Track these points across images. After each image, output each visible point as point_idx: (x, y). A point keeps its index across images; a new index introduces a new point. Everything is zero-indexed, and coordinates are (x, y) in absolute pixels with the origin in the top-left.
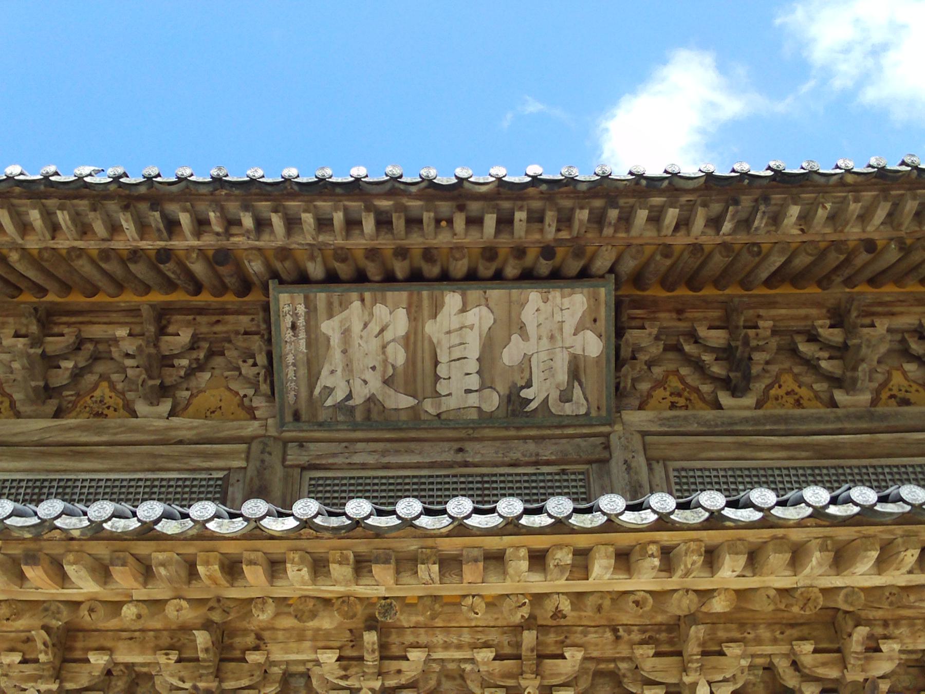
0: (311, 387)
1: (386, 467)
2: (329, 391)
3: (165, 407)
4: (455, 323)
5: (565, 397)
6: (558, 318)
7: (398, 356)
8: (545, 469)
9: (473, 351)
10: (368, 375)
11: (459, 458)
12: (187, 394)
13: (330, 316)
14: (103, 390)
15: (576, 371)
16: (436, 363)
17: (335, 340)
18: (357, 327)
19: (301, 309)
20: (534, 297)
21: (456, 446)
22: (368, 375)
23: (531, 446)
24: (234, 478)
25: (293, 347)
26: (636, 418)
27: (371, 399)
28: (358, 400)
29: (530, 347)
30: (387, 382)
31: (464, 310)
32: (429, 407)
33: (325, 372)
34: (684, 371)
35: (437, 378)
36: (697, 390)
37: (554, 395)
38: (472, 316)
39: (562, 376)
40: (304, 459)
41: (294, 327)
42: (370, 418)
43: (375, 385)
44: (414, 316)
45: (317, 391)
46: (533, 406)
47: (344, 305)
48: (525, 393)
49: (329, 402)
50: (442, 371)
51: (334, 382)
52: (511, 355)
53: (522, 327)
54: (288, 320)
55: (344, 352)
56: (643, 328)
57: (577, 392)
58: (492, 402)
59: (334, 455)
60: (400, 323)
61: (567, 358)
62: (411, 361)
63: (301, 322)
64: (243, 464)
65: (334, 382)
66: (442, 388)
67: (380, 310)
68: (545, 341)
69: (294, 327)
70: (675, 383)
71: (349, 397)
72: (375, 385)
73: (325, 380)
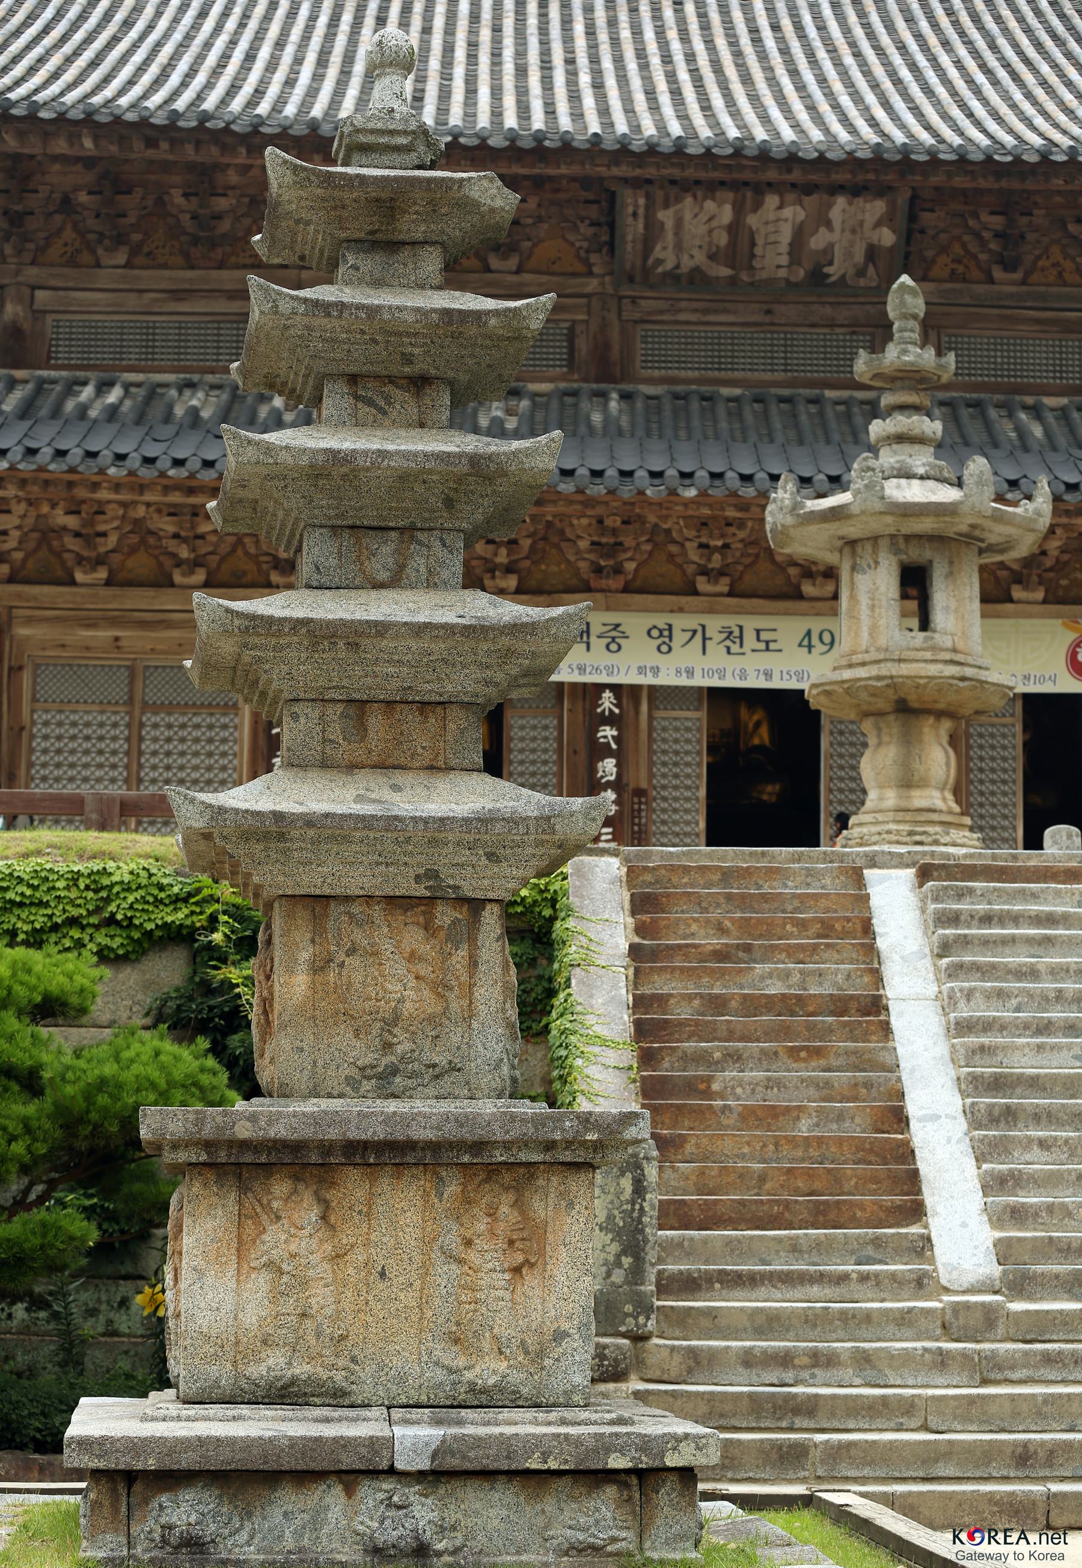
0: (645, 258)
1: (708, 323)
2: (659, 262)
3: (513, 263)
4: (772, 217)
5: (861, 273)
6: (860, 217)
7: (723, 239)
8: (838, 330)
9: (786, 236)
10: (695, 252)
11: (767, 319)
12: (528, 244)
13: (666, 206)
16: (753, 244)
17: (669, 224)
18: (688, 216)
19: (642, 201)
20: (841, 201)
21: (765, 307)
22: (695, 252)
23: (828, 310)
24: (579, 329)
25: (633, 229)
27: (696, 270)
28: (684, 269)
29: (835, 237)
30: (711, 257)
31: (781, 207)
32: (745, 277)
33: (658, 248)
34: (967, 238)
35: (753, 256)
36: (975, 257)
37: (851, 272)
38: (788, 212)
39: (859, 257)
40: (637, 316)
41: (635, 215)
43: (700, 258)
44: (739, 210)
45: (650, 261)
46: (833, 279)
47: (678, 200)
48: (826, 270)
49: (660, 270)
50: (758, 251)
51: (665, 255)
52: (818, 241)
53: (829, 224)
54: (630, 210)
55: (676, 234)
56: (932, 210)
57: (871, 270)
59: (662, 312)
60: (726, 214)
61: (864, 245)
62: (733, 243)
63: (641, 211)
64: (584, 317)
65: (665, 255)
66: (756, 263)
67: (710, 205)
68: (847, 233)
69: (635, 215)
70: (957, 249)
71: (678, 267)
72: (700, 258)
73: (658, 252)
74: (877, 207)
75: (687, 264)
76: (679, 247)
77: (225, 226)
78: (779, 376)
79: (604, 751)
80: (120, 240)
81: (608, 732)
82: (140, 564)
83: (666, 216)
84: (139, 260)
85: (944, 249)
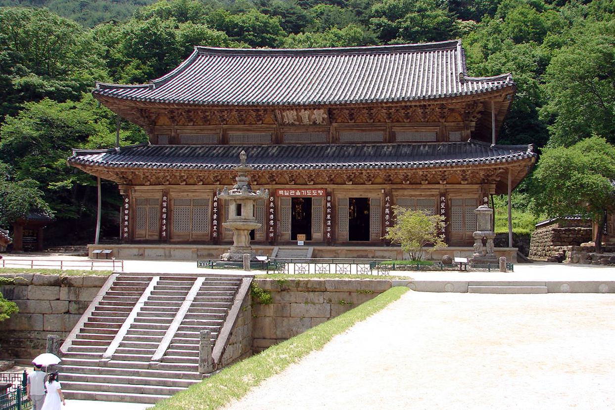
5: (323, 122)
9: (307, 117)
14: (251, 118)
15: (323, 119)
18: (288, 114)
25: (279, 116)
26: (335, 125)
32: (302, 124)
42: (293, 124)
51: (286, 120)
52: (313, 117)
58: (311, 123)
60: (295, 113)
62: (298, 118)
70: (342, 116)
74: (322, 111)
75: (290, 122)
76: (288, 119)
77: (209, 117)
78: (309, 142)
79: (271, 213)
80: (192, 120)
81: (272, 210)
82: (191, 181)
83: (284, 114)
84: (195, 124)
85: (340, 117)
